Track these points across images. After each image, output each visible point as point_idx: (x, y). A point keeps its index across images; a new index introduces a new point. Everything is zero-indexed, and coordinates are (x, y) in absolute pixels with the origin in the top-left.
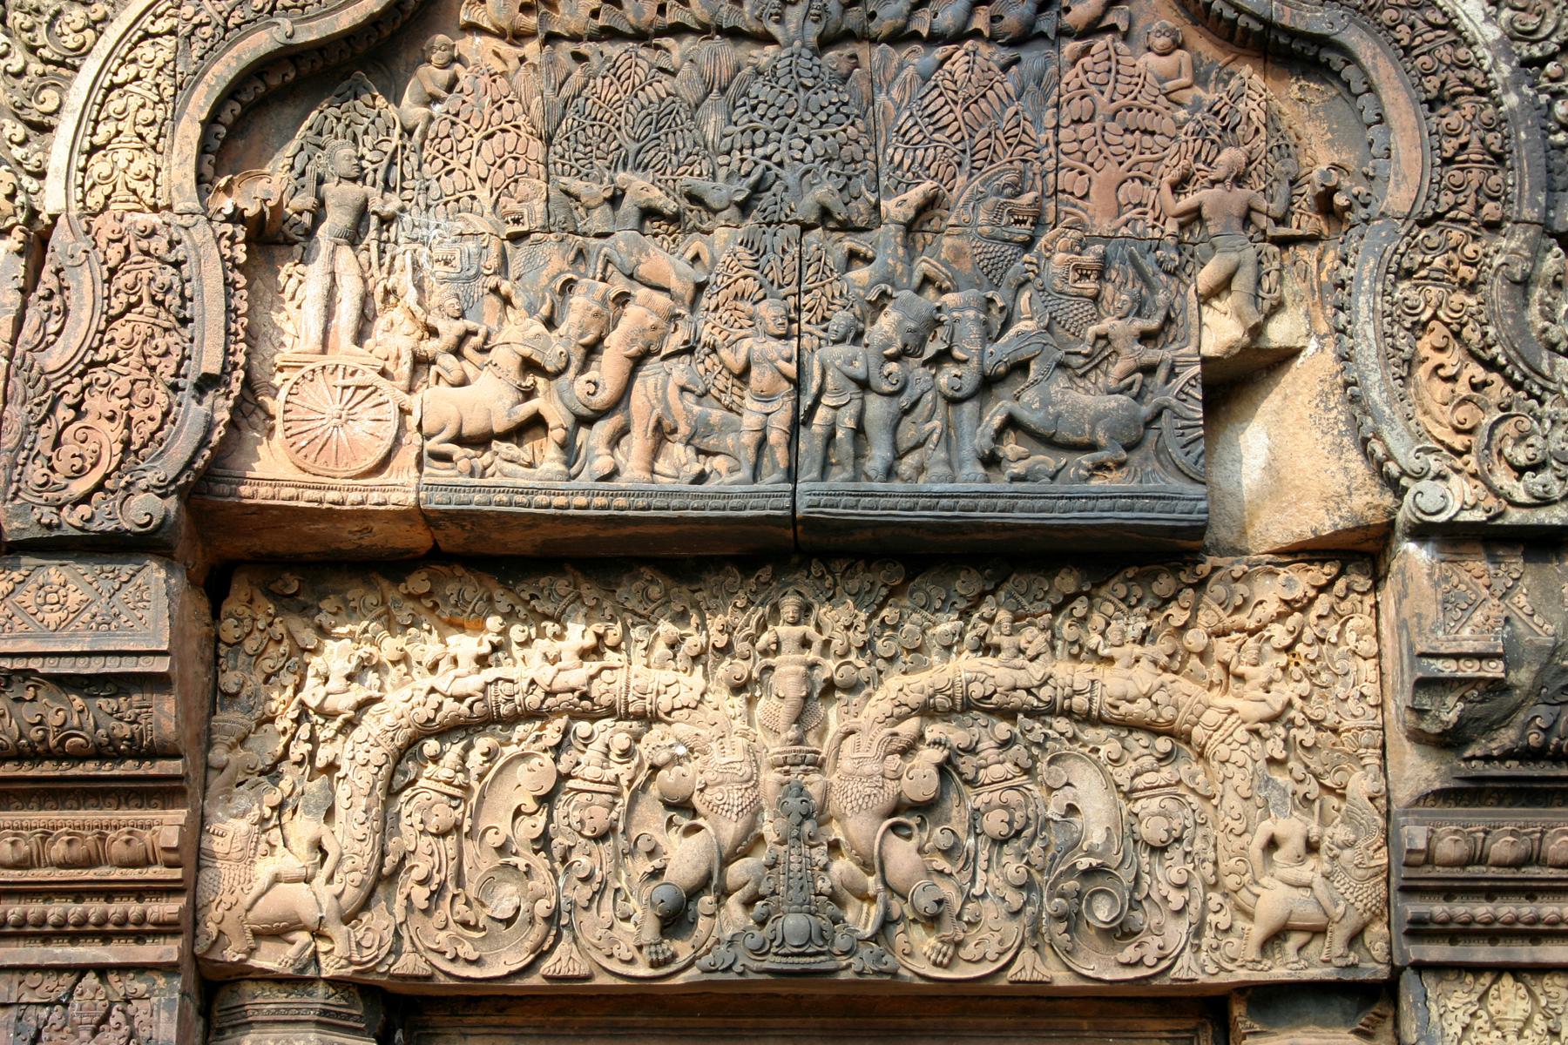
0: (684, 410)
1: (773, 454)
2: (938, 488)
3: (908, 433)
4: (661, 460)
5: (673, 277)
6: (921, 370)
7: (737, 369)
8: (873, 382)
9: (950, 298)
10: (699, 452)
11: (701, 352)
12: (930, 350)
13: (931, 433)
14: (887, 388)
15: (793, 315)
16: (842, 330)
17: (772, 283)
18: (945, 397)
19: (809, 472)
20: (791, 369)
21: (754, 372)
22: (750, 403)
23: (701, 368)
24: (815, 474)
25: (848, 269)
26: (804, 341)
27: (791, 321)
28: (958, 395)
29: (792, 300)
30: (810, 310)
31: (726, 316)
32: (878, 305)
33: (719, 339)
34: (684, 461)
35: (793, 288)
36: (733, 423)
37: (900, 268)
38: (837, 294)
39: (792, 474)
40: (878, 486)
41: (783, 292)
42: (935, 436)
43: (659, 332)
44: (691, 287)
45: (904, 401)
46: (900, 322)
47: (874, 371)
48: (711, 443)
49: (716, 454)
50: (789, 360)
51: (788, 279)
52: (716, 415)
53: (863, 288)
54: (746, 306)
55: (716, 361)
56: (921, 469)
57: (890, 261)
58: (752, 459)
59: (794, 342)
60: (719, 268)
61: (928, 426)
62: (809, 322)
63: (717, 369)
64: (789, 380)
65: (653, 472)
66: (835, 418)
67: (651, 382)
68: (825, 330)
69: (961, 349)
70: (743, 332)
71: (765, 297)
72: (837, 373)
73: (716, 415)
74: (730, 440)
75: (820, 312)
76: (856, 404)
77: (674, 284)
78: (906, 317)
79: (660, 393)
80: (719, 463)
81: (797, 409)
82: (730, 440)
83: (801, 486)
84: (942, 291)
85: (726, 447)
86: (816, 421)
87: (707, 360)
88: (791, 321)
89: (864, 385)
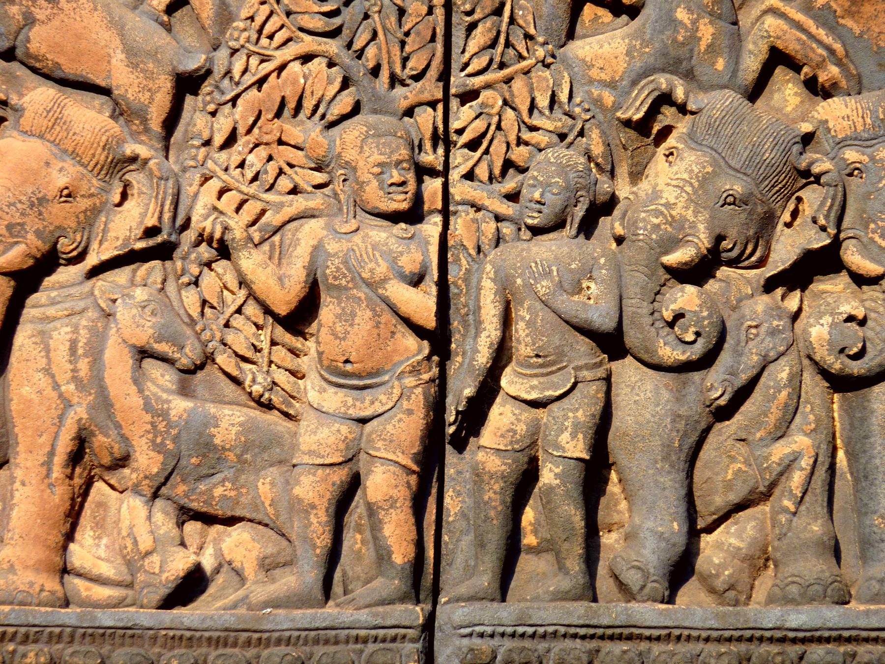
0: (146, 407)
1: (376, 527)
2: (799, 618)
3: (726, 466)
4: (85, 534)
5: (118, 58)
6: (763, 302)
7: (284, 300)
8: (632, 338)
9: (837, 113)
10: (186, 514)
11: (190, 256)
12: (785, 249)
13: (787, 468)
14: (670, 353)
15: (431, 157)
16: (554, 200)
17: (375, 71)
18: (824, 373)
19: (470, 572)
20: (422, 304)
21: (328, 312)
22: (315, 391)
23: (191, 298)
24: (485, 579)
25: (571, 35)
26: (459, 226)
27: (422, 172)
28: (857, 368)
29: (426, 119)
30: (473, 145)
31: (255, 160)
32: (647, 129)
33: (237, 224)
34: (145, 543)
35: (430, 88)
36: (275, 440)
37: (707, 32)
38: (543, 102)
39: (422, 579)
40: (648, 613)
41: (403, 96)
42: (797, 479)
43: (83, 204)
44: (165, 85)
45: (716, 384)
46: (705, 181)
47: (637, 306)
48: (219, 492)
49: (231, 521)
50: (417, 281)
51: (416, 64)
52: (230, 420)
53: (611, 85)
54: (305, 131)
55: (231, 280)
56: (760, 560)
57: (681, 14)
58: (323, 540)
59: (432, 227)
60: (239, 32)
61: (780, 451)
62: (470, 176)
63: (233, 301)
64: (419, 331)
65: (65, 571)
66: (535, 430)
67: (61, 335)
68: (513, 197)
69: (866, 249)
70: (299, 203)
71: (356, 110)
72: (543, 314)
73: (230, 420)
74: (266, 486)
75: (498, 150)
76: (593, 391)
77: (122, 77)
78: (722, 164)
79: (83, 366)
80: (239, 544)
81: (437, 406)
82: (266, 486)
83: (451, 613)
84: (816, 89)
85: (256, 505)
86: (488, 436)
87: (209, 280)
88: (422, 172)
89: (612, 343)
